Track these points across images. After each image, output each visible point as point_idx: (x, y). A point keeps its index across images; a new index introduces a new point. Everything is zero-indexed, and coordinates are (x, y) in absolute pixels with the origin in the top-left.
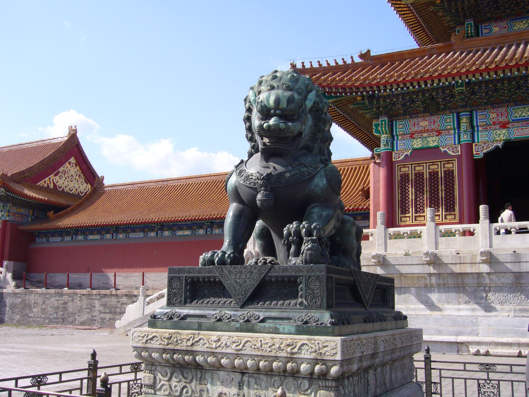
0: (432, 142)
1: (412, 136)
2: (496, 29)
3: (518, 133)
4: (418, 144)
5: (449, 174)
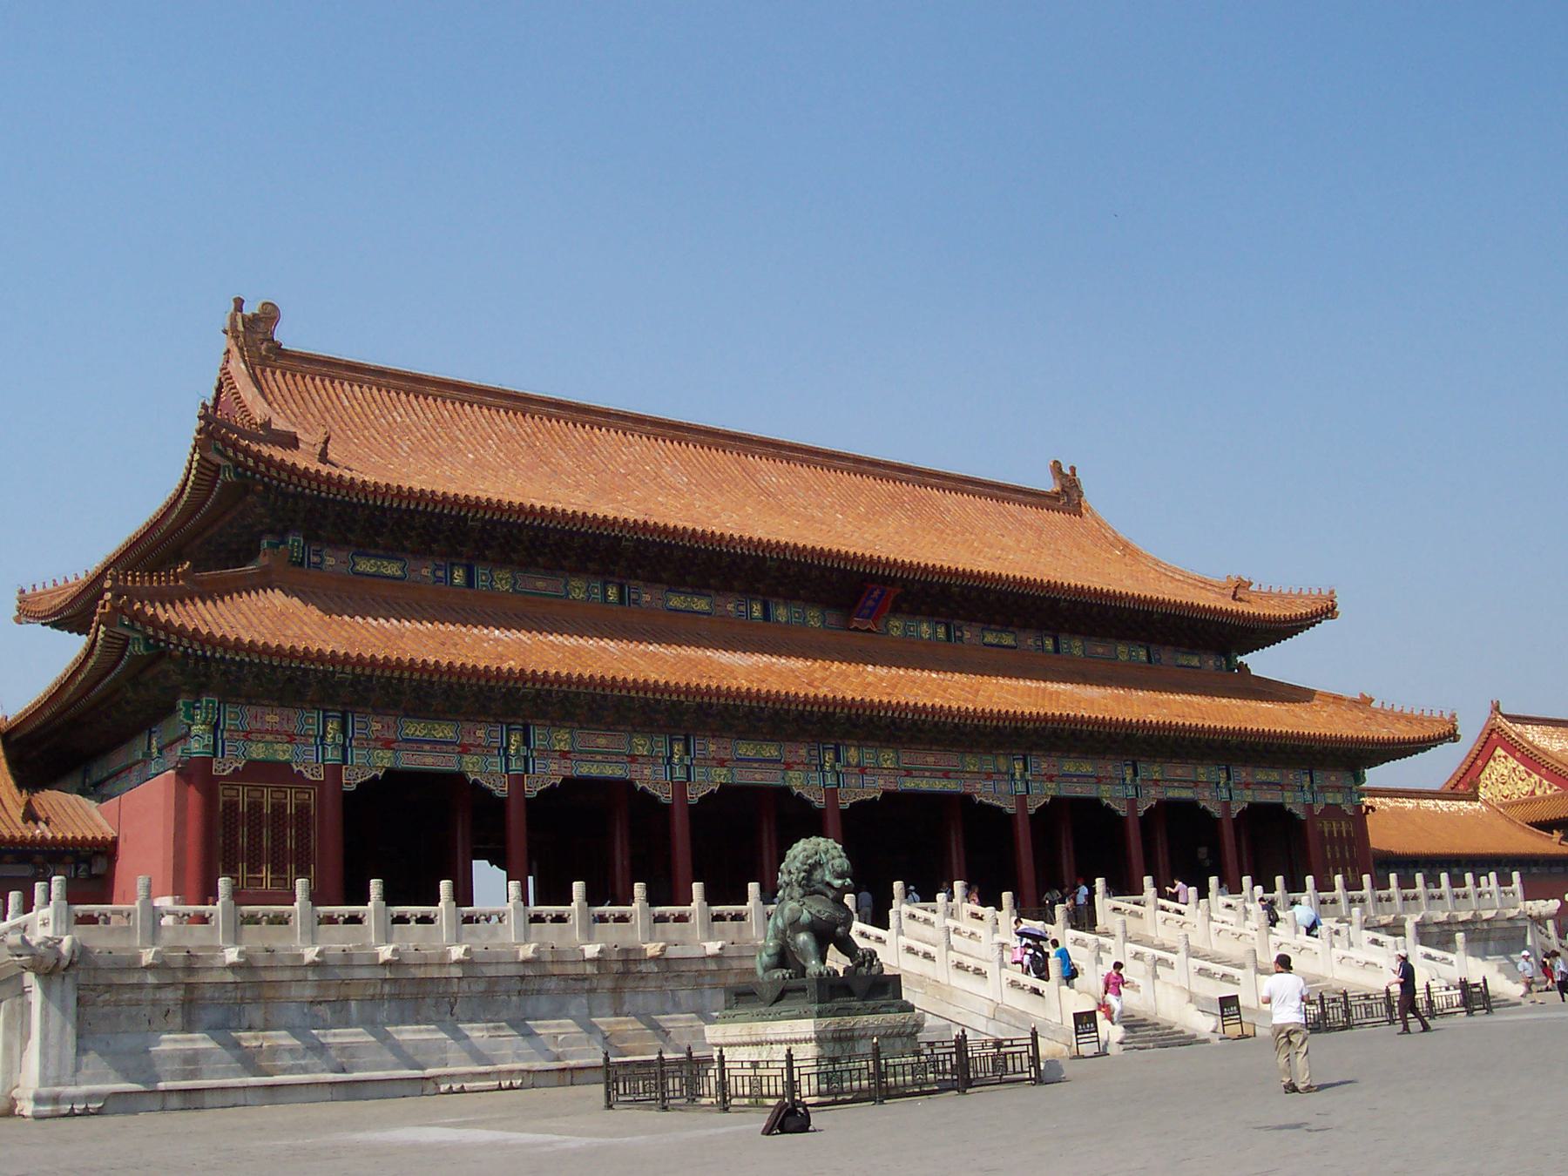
0: (283, 753)
1: (247, 736)
2: (331, 561)
3: (409, 761)
4: (258, 752)
5: (302, 809)
